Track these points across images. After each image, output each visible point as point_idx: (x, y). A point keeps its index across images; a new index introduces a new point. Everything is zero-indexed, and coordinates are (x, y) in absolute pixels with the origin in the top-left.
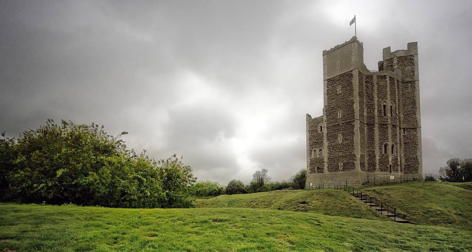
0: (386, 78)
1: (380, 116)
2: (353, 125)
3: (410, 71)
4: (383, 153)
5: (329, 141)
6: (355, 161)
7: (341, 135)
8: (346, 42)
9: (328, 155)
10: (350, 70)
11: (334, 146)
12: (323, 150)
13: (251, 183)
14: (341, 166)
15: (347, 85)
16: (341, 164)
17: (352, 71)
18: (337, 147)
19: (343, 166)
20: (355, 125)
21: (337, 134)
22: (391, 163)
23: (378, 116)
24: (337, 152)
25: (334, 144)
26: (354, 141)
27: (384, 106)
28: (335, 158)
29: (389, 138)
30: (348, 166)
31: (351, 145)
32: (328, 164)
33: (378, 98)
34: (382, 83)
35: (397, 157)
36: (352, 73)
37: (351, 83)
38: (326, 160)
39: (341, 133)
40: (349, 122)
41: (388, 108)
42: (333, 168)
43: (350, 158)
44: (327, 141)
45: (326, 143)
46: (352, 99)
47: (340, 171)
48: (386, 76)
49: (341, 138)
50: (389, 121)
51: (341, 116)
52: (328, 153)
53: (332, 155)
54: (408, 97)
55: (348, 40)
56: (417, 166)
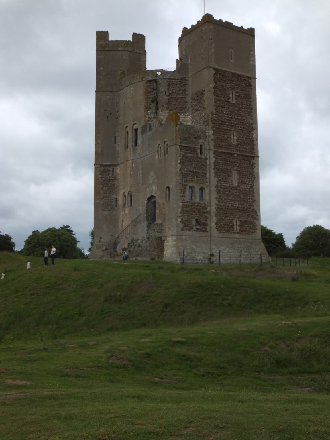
2: (253, 163)
5: (217, 177)
8: (242, 27)
9: (217, 202)
11: (226, 188)
13: (90, 233)
14: (236, 225)
15: (244, 97)
16: (237, 223)
18: (230, 192)
19: (239, 226)
20: (255, 164)
21: (231, 170)
24: (230, 199)
25: (225, 185)
26: (254, 189)
28: (228, 209)
30: (245, 226)
32: (217, 218)
36: (250, 81)
38: (213, 209)
39: (236, 170)
40: (247, 156)
43: (248, 215)
44: (215, 177)
45: (212, 179)
49: (237, 179)
51: (236, 143)
52: (216, 198)
53: (222, 203)
55: (246, 27)
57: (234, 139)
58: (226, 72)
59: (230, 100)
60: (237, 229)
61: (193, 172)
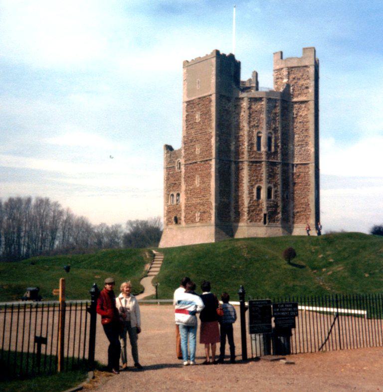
0: (263, 101)
1: (250, 151)
3: (303, 87)
4: (255, 198)
6: (211, 211)
7: (198, 176)
10: (209, 93)
12: (181, 195)
16: (198, 214)
17: (211, 95)
22: (265, 211)
23: (249, 152)
27: (259, 138)
29: (263, 178)
31: (207, 189)
33: (250, 128)
34: (257, 106)
35: (277, 203)
36: (210, 97)
37: (210, 110)
38: (183, 208)
39: (199, 174)
40: (207, 160)
41: (263, 140)
42: (190, 220)
46: (210, 131)
47: (197, 222)
48: (263, 98)
50: (264, 157)
51: (199, 152)
54: (300, 122)
56: (309, 213)
57: (198, 151)
58: (194, 100)
59: (197, 121)
60: (197, 220)
61: (173, 184)
